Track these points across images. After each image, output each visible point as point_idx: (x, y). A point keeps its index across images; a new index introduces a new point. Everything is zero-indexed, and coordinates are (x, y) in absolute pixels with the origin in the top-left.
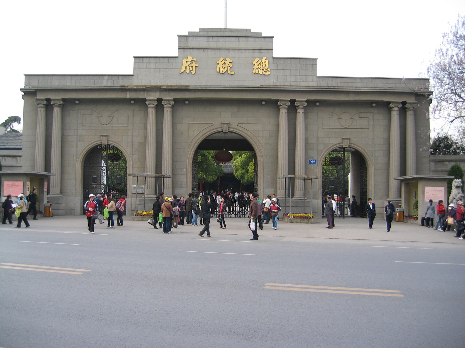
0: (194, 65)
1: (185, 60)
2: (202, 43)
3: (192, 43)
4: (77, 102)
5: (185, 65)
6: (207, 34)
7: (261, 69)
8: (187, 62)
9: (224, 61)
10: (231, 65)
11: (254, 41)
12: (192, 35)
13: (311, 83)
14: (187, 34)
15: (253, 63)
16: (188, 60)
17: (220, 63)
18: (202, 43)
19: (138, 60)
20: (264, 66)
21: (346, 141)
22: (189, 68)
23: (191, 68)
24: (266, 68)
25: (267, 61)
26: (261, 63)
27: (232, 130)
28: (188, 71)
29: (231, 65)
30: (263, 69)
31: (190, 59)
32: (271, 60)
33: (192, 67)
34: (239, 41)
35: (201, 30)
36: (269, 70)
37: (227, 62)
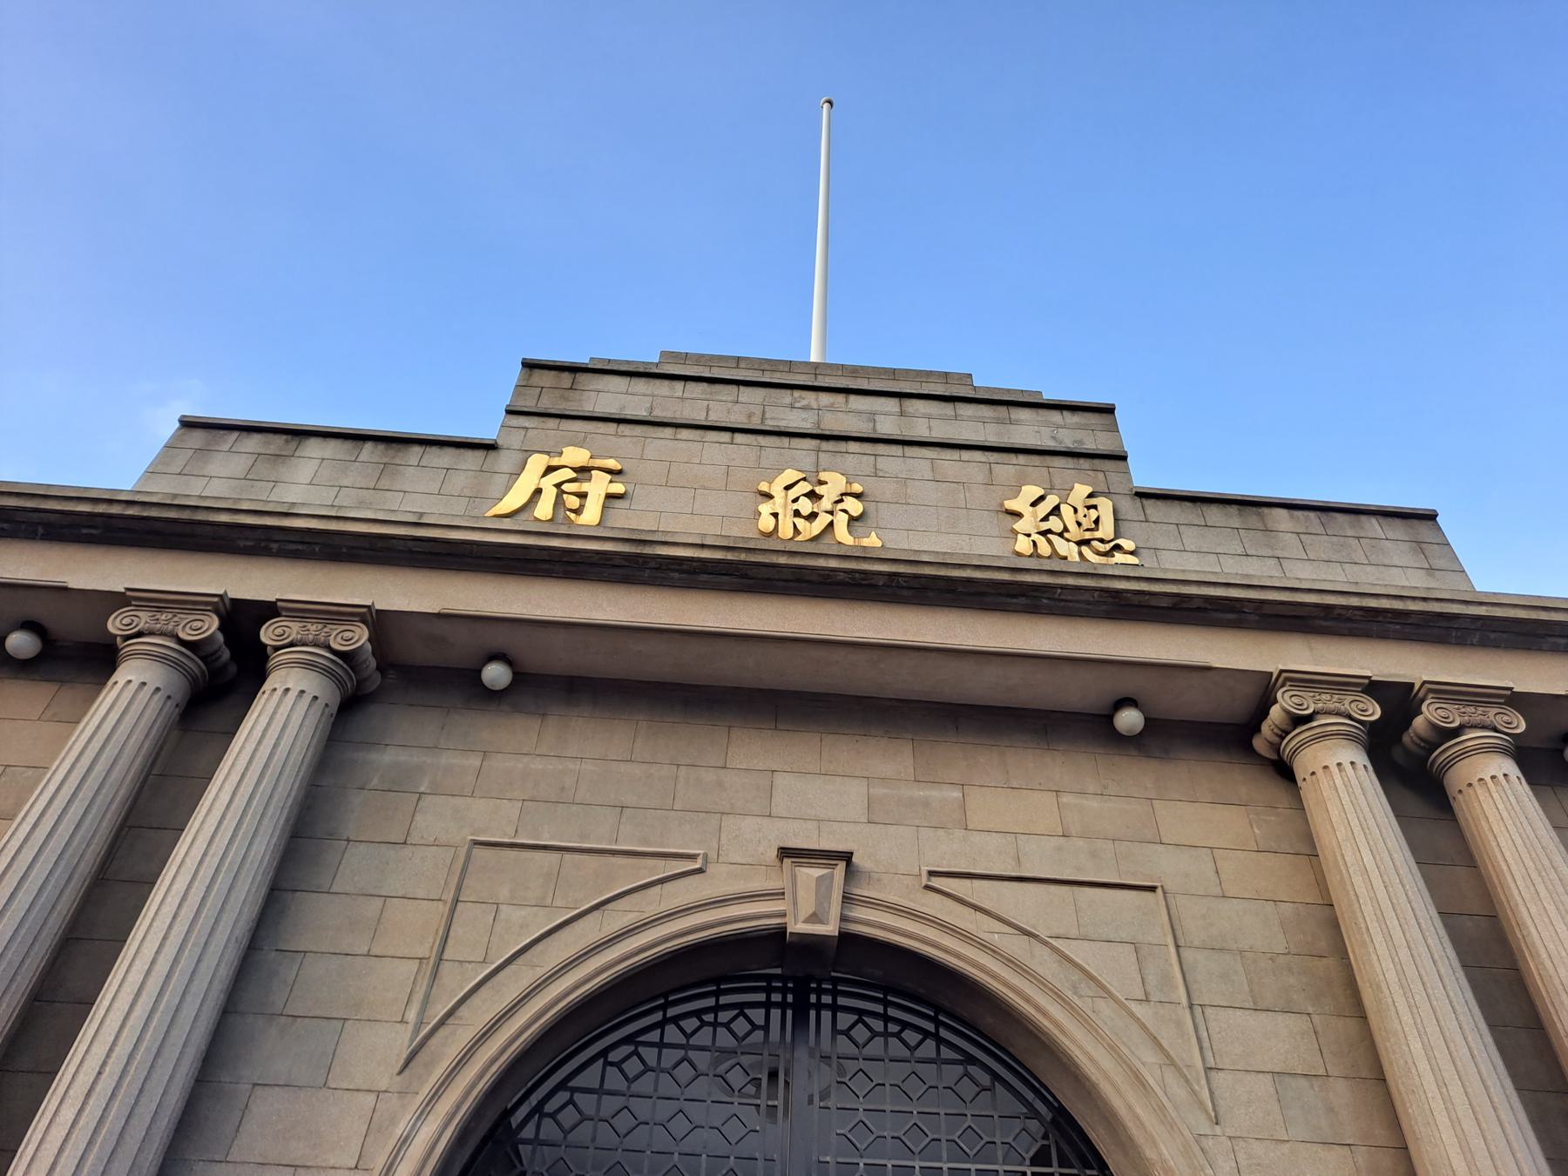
0: (598, 486)
7: (1075, 533)
8: (550, 469)
9: (805, 487)
10: (855, 507)
11: (999, 421)
15: (1011, 505)
16: (555, 462)
17: (777, 490)
19: (198, 437)
20: (1086, 524)
22: (559, 501)
23: (573, 502)
24: (1106, 530)
26: (1066, 510)
27: (873, 923)
28: (544, 509)
29: (855, 507)
30: (1086, 542)
31: (576, 456)
33: (583, 496)
34: (902, 414)
35: (668, 356)
36: (1127, 544)
37: (829, 493)
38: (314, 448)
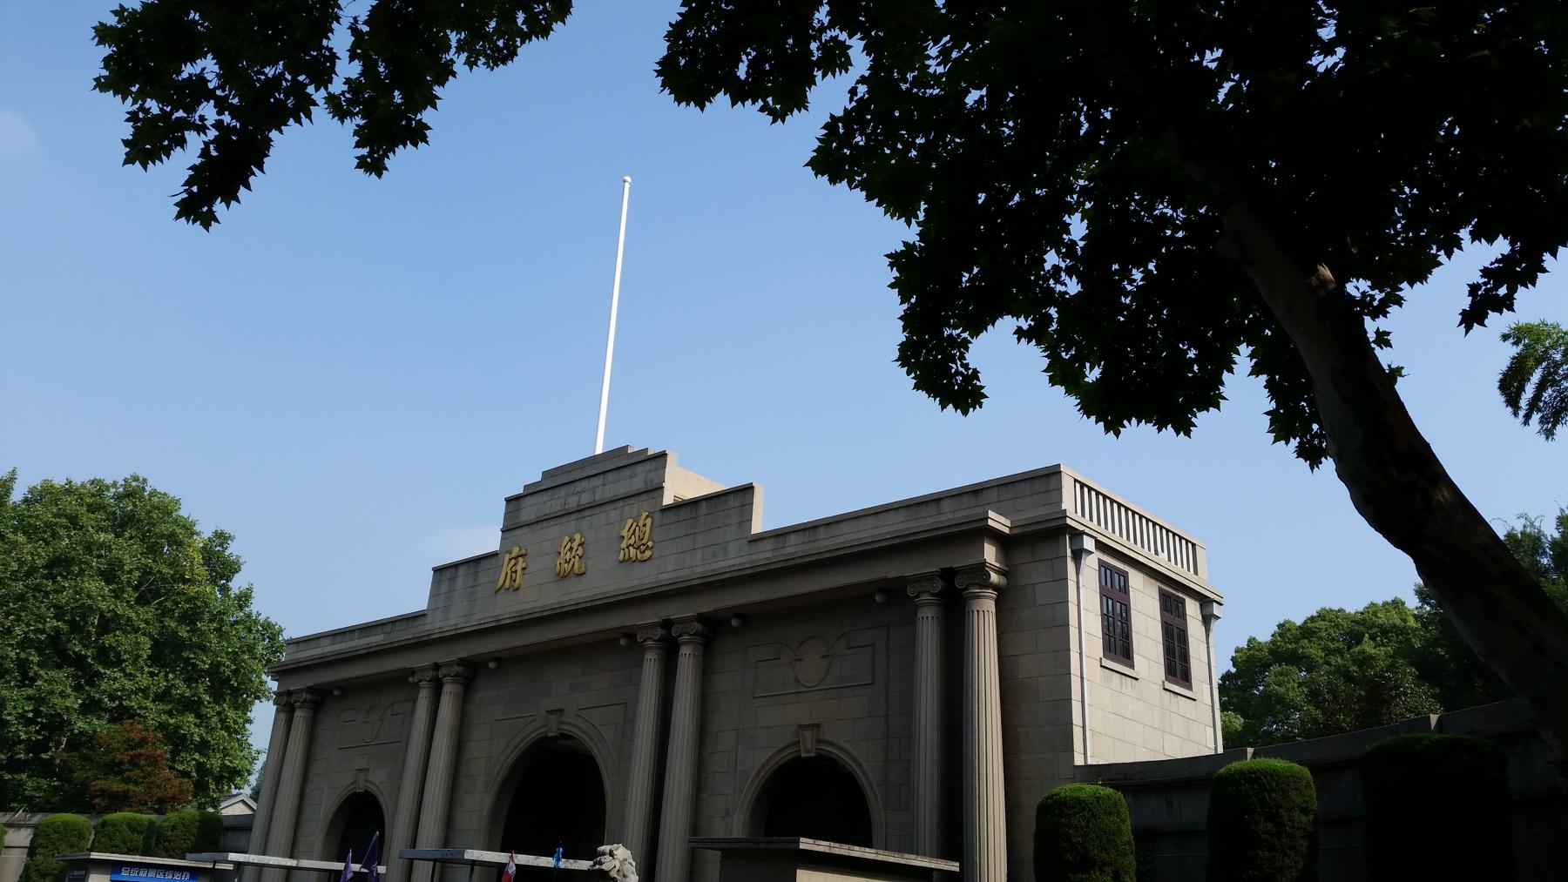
1: (507, 557)
2: (552, 504)
3: (528, 512)
4: (336, 693)
5: (506, 569)
6: (557, 480)
12: (532, 491)
13: (734, 559)
14: (520, 491)
18: (552, 504)
21: (808, 734)
25: (649, 521)
29: (580, 552)
31: (516, 551)
32: (657, 516)
35: (546, 474)
38: (462, 571)
